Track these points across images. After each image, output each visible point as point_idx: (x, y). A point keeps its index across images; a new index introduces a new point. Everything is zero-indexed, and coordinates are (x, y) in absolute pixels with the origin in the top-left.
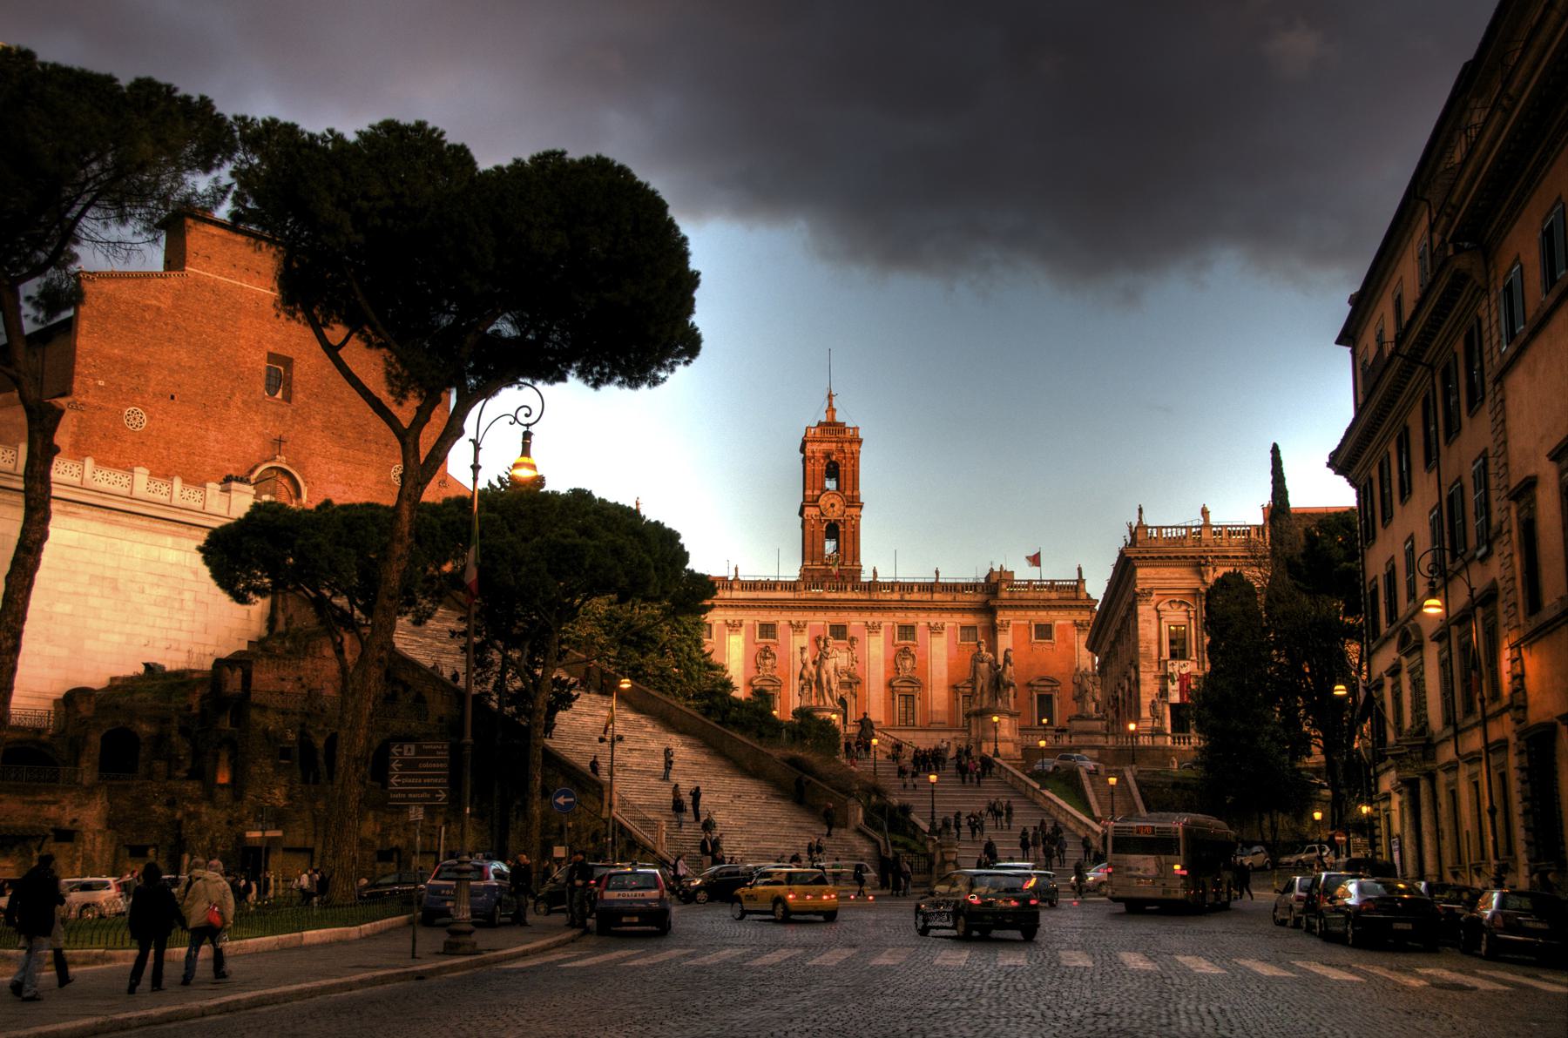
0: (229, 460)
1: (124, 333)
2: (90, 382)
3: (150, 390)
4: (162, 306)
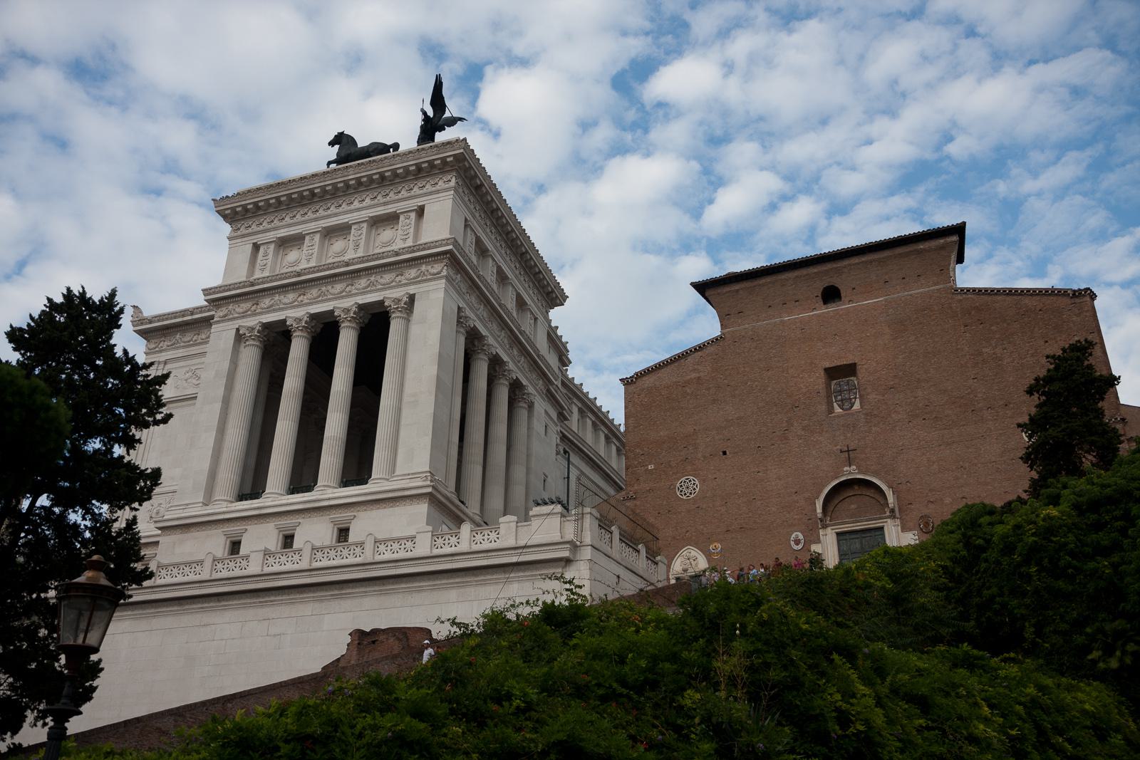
0: (796, 493)
1: (668, 414)
3: (700, 455)
4: (702, 374)
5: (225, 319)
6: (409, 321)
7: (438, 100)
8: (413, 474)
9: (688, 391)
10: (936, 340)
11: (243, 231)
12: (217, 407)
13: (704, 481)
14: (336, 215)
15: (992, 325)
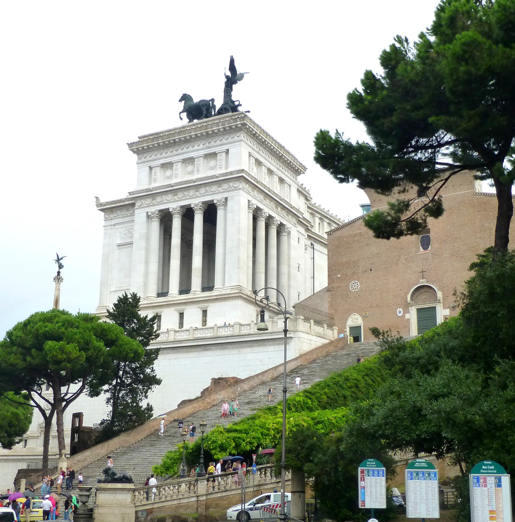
1: (347, 250)
2: (334, 277)
3: (360, 271)
4: (362, 231)
5: (140, 207)
6: (225, 209)
7: (232, 67)
8: (232, 286)
9: (356, 239)
10: (466, 218)
11: (143, 160)
12: (143, 252)
13: (362, 283)
14: (187, 153)
15: (490, 212)
